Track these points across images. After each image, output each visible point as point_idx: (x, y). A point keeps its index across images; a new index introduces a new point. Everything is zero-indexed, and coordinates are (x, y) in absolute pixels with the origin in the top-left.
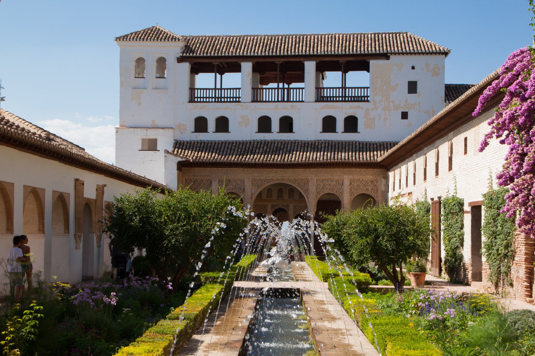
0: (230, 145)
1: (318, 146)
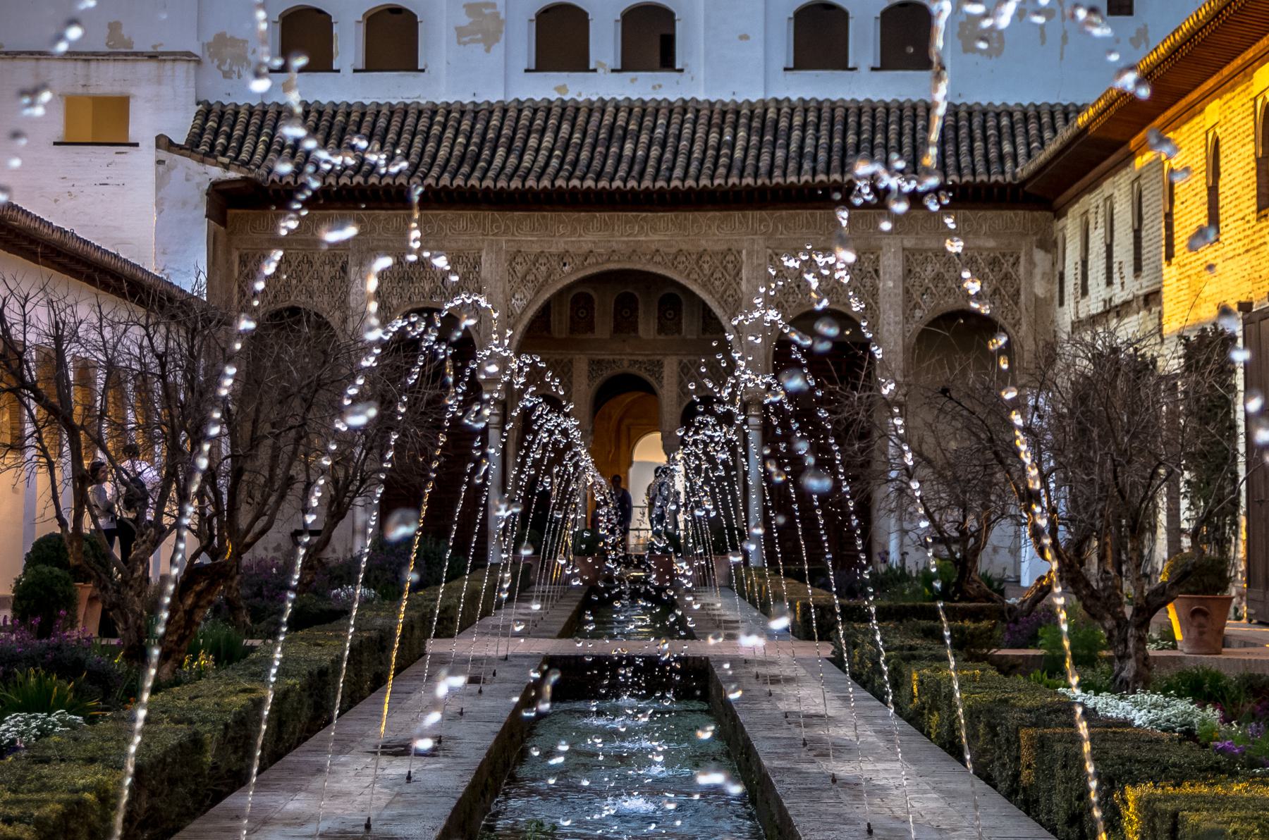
0: (424, 122)
1: (777, 122)
